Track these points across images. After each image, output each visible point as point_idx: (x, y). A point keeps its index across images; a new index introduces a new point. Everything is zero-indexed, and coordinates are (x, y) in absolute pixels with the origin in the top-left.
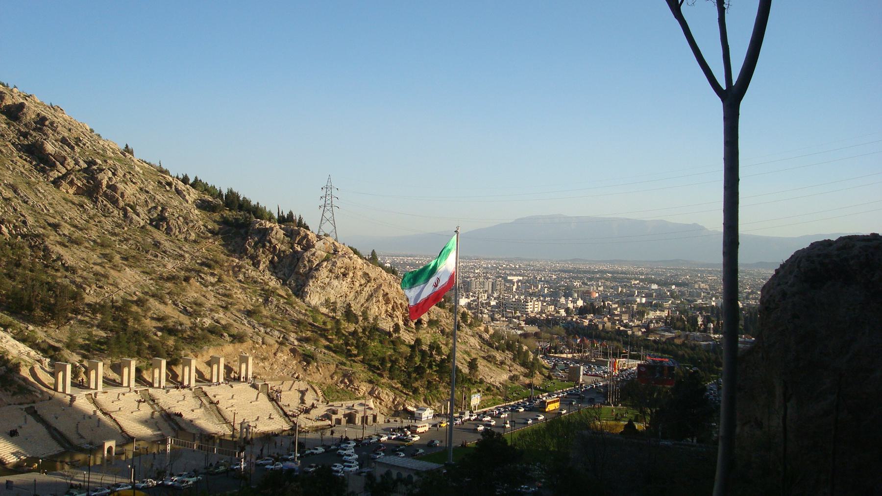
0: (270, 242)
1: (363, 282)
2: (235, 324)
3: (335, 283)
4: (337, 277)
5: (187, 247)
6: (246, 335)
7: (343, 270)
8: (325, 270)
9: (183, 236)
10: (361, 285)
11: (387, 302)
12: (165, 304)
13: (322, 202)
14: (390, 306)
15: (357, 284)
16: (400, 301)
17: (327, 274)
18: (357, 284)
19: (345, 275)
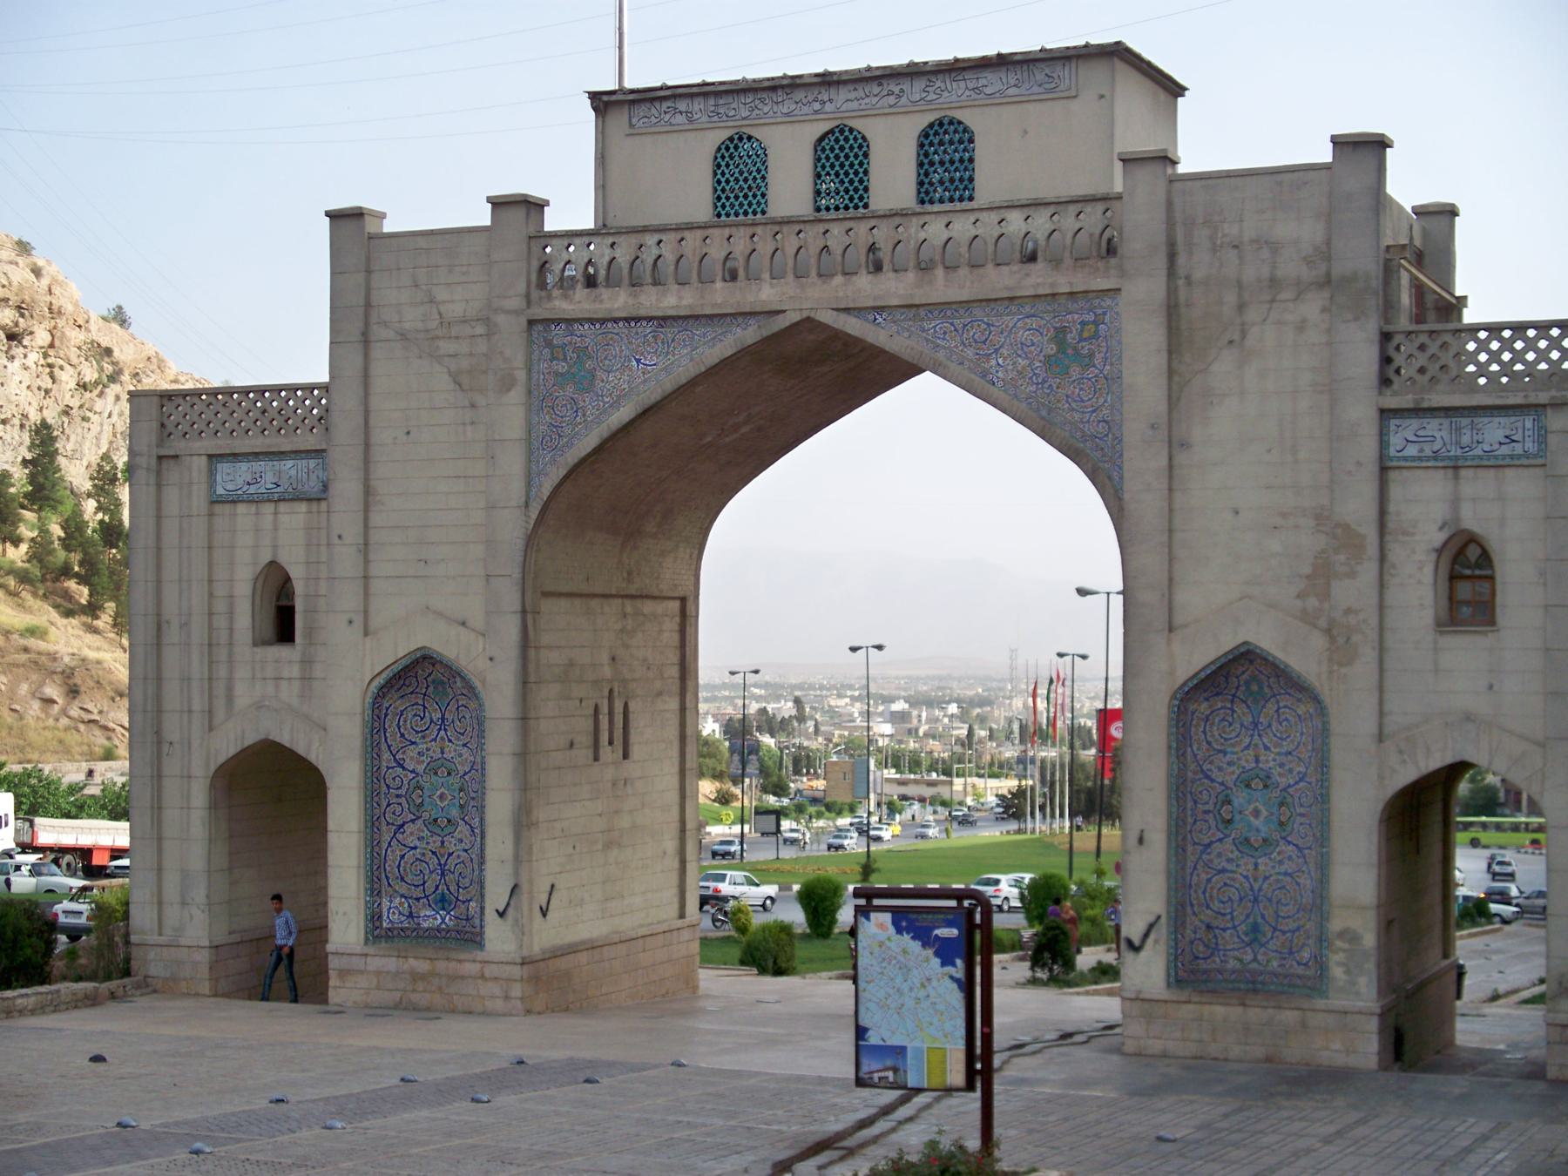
1: (90, 374)
15: (67, 378)
18: (67, 378)
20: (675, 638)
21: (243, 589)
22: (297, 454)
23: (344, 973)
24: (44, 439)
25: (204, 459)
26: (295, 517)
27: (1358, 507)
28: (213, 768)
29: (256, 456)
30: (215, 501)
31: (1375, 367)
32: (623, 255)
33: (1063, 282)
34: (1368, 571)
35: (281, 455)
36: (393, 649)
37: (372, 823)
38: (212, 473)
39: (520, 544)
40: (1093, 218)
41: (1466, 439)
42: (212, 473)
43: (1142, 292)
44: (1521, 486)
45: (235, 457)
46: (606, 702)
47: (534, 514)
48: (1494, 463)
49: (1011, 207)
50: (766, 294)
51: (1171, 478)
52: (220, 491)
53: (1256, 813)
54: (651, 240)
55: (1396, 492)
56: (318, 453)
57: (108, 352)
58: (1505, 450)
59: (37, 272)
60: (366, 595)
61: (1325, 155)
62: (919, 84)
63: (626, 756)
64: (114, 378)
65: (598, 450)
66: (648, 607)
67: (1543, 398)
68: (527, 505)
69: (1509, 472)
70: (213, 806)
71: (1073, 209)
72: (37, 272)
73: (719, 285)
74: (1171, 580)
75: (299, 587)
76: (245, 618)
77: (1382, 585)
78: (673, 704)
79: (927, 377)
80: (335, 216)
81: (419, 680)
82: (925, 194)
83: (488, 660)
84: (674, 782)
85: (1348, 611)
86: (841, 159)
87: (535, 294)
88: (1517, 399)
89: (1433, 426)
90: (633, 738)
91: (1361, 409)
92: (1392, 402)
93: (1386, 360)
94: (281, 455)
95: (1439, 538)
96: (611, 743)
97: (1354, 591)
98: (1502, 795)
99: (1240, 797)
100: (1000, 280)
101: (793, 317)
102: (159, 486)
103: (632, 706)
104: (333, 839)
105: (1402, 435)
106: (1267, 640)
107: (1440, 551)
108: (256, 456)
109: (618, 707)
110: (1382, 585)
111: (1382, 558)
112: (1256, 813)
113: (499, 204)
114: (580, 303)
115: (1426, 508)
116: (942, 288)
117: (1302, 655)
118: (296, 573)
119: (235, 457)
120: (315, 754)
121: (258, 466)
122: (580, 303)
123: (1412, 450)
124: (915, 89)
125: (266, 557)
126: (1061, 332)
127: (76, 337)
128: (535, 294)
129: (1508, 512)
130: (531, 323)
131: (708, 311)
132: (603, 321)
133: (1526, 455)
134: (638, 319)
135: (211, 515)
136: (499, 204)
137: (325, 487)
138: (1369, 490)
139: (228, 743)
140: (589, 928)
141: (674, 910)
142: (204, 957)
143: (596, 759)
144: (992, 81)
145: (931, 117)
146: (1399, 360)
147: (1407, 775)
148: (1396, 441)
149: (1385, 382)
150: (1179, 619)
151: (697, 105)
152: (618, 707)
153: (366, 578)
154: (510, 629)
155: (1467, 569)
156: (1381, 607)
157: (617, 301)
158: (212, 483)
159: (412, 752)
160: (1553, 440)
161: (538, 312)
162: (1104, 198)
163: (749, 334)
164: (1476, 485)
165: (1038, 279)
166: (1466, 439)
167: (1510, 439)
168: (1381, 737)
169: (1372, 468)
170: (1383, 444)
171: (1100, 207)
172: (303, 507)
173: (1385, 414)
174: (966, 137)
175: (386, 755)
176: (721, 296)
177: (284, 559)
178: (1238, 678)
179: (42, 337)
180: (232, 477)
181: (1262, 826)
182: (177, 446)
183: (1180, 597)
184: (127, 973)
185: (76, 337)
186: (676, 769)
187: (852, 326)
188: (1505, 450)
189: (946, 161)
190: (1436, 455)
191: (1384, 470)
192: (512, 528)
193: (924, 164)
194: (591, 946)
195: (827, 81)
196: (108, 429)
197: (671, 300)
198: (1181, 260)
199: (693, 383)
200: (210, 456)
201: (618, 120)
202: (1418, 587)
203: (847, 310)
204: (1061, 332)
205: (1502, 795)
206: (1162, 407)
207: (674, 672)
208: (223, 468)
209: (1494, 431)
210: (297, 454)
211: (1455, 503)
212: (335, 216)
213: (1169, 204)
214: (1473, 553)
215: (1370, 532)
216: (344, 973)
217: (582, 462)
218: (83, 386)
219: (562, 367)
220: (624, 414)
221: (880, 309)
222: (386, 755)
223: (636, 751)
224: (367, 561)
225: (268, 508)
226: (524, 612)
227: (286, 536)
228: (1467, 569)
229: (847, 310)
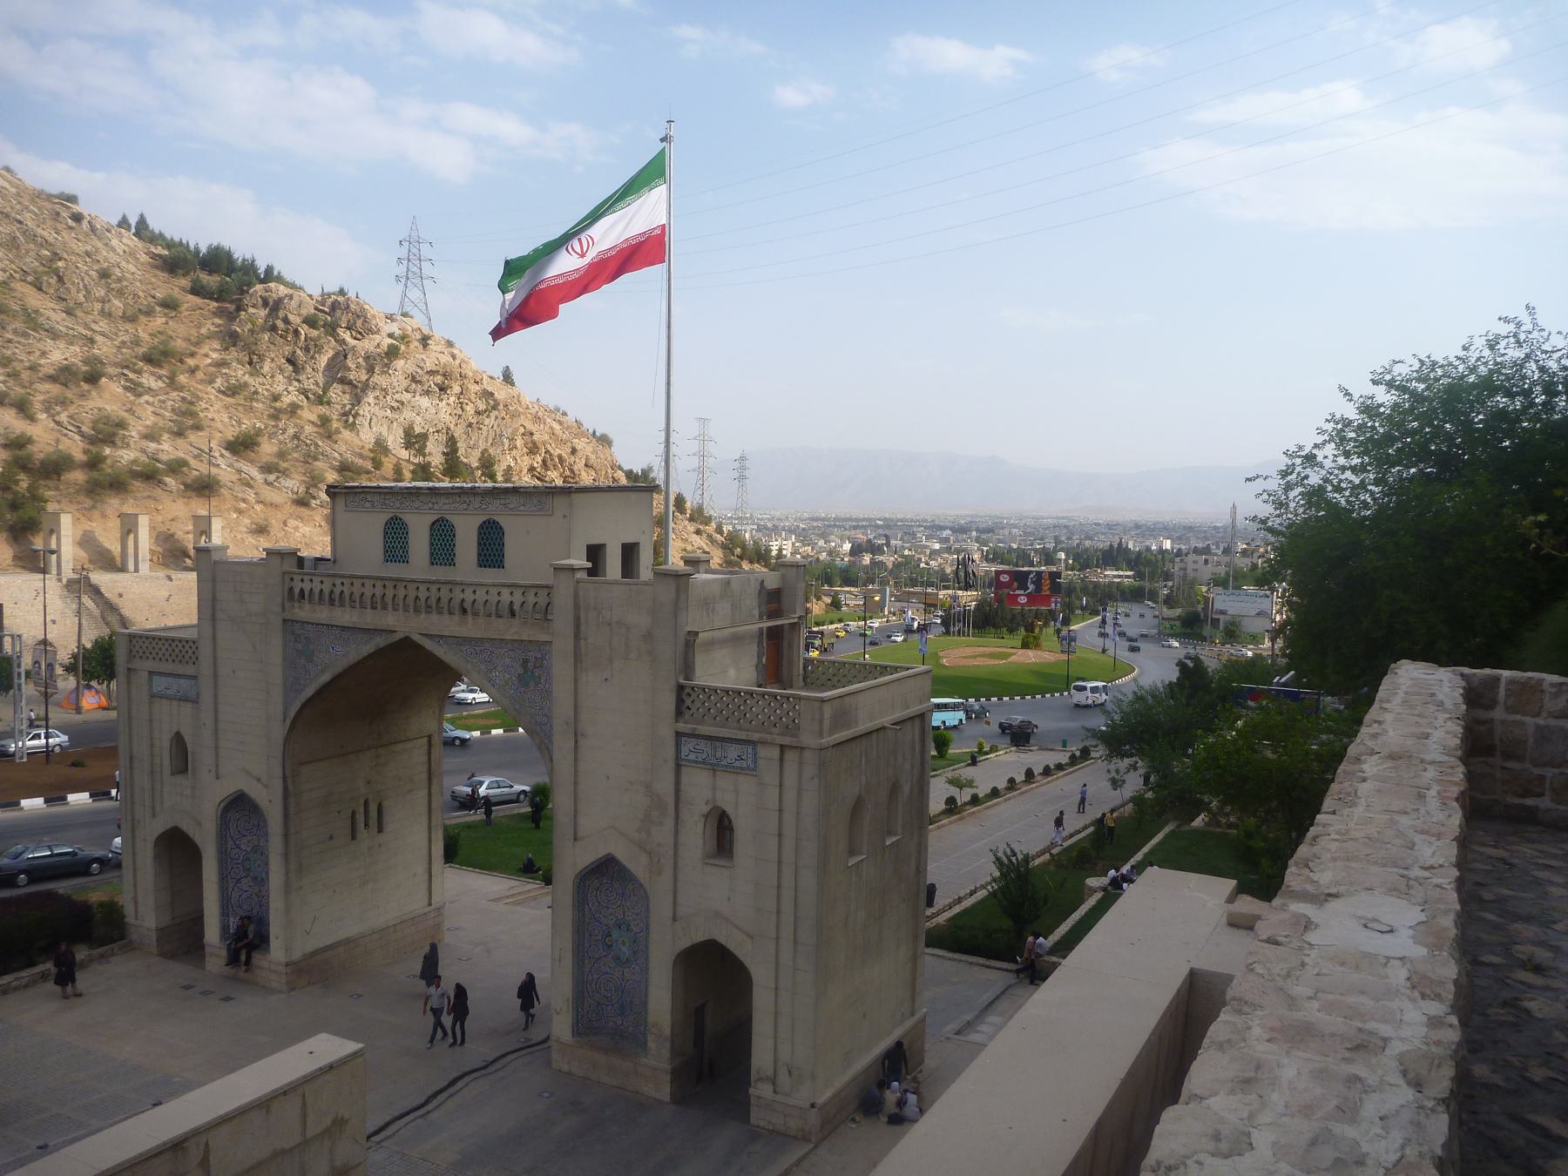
0: (286, 321)
1: (482, 407)
2: (193, 462)
3: (424, 402)
4: (427, 393)
5: (103, 325)
6: (218, 482)
7: (439, 379)
8: (401, 377)
9: (98, 306)
10: (478, 413)
11: (533, 449)
12: (31, 418)
13: (402, 270)
14: (539, 459)
15: (470, 409)
16: (558, 452)
17: (405, 383)
18: (470, 409)
19: (442, 389)
20: (425, 758)
21: (166, 744)
23: (212, 955)
24: (452, 442)
26: (187, 709)
27: (665, 786)
29: (169, 675)
30: (153, 696)
31: (673, 707)
32: (327, 588)
33: (527, 634)
34: (669, 823)
35: (179, 676)
36: (227, 788)
37: (223, 878)
38: (150, 680)
39: (281, 741)
40: (542, 599)
41: (718, 755)
42: (150, 680)
43: (562, 646)
44: (746, 784)
45: (160, 674)
46: (362, 809)
48: (731, 769)
49: (504, 586)
50: (390, 620)
51: (576, 753)
53: (624, 943)
54: (338, 582)
55: (684, 779)
56: (194, 678)
57: (492, 394)
58: (737, 764)
59: (454, 357)
60: (217, 755)
62: (478, 499)
63: (380, 830)
64: (494, 408)
65: (314, 696)
66: (400, 747)
67: (756, 736)
69: (741, 778)
70: (157, 857)
71: (533, 591)
72: (454, 357)
73: (369, 611)
74: (576, 811)
77: (676, 832)
78: (424, 793)
81: (239, 806)
83: (269, 799)
84: (425, 834)
85: (659, 845)
86: (442, 535)
87: (287, 604)
89: (702, 744)
90: (386, 819)
91: (666, 731)
92: (681, 727)
93: (680, 701)
94: (179, 676)
95: (706, 809)
96: (366, 825)
97: (662, 834)
99: (615, 934)
101: (402, 636)
102: (129, 683)
103: (386, 804)
104: (205, 885)
105: (688, 746)
106: (621, 856)
107: (706, 816)
108: (169, 675)
109: (373, 808)
110: (676, 832)
111: (677, 818)
112: (624, 943)
114: (304, 612)
117: (637, 865)
118: (188, 739)
119: (160, 674)
120: (197, 839)
122: (304, 612)
123: (692, 757)
124: (476, 502)
125: (175, 730)
126: (525, 662)
127: (474, 388)
128: (287, 604)
129: (742, 798)
133: (748, 768)
135: (151, 703)
138: (671, 778)
139: (159, 826)
140: (351, 929)
141: (426, 902)
142: (154, 935)
143: (353, 838)
144: (514, 501)
145: (485, 518)
146: (688, 702)
149: (679, 713)
150: (581, 833)
151: (376, 498)
152: (373, 808)
153: (217, 748)
154: (278, 785)
155: (722, 830)
156: (676, 844)
157: (322, 614)
159: (245, 840)
160: (761, 763)
161: (288, 616)
162: (547, 587)
163: (381, 641)
164: (725, 781)
165: (511, 630)
166: (718, 755)
168: (674, 919)
169: (671, 764)
171: (546, 591)
172: (190, 705)
173: (678, 735)
175: (230, 842)
176: (369, 619)
179: (457, 389)
180: (160, 684)
181: (625, 951)
182: (137, 664)
183: (582, 821)
184: (122, 938)
185: (474, 388)
186: (426, 826)
187: (428, 644)
188: (737, 764)
189: (491, 547)
190: (704, 762)
191: (678, 767)
192: (279, 732)
193: (482, 543)
194: (348, 941)
196: (492, 434)
197: (346, 617)
198: (583, 628)
199: (359, 663)
201: (340, 501)
202: (696, 837)
203: (426, 635)
204: (525, 662)
206: (572, 714)
207: (424, 776)
208: (156, 678)
209: (733, 752)
211: (714, 788)
213: (576, 596)
215: (670, 800)
216: (212, 955)
217: (310, 700)
218: (478, 413)
219: (299, 646)
220: (326, 677)
221: (442, 637)
222: (230, 842)
223: (389, 826)
224: (217, 740)
225: (175, 703)
226: (285, 778)
228: (722, 830)
229: (426, 635)
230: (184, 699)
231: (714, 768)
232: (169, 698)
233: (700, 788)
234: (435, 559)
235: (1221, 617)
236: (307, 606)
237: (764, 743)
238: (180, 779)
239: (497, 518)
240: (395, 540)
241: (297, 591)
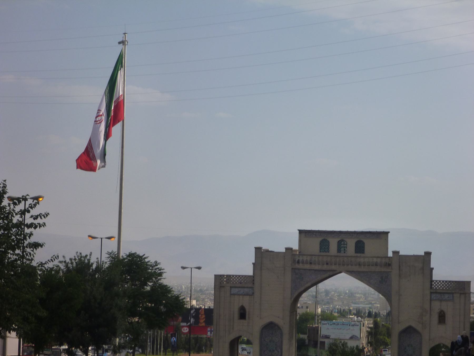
22: (247, 287)
25: (229, 288)
26: (247, 298)
28: (230, 341)
29: (239, 287)
30: (231, 294)
33: (383, 269)
36: (266, 321)
38: (231, 290)
47: (293, 299)
49: (374, 257)
52: (232, 293)
54: (314, 257)
61: (423, 254)
67: (453, 292)
68: (291, 298)
75: (247, 310)
76: (236, 315)
79: (343, 274)
80: (256, 248)
81: (271, 327)
82: (356, 252)
88: (450, 292)
92: (432, 291)
94: (244, 287)
98: (307, 341)
100: (373, 269)
105: (434, 296)
106: (413, 325)
108: (239, 287)
111: (430, 314)
113: (287, 249)
114: (301, 266)
115: (437, 306)
116: (362, 269)
117: (419, 327)
118: (247, 308)
121: (240, 289)
122: (301, 266)
123: (435, 298)
125: (241, 305)
129: (448, 307)
130: (292, 269)
131: (324, 269)
132: (305, 269)
134: (311, 270)
136: (287, 249)
137: (253, 293)
145: (358, 240)
147: (433, 345)
148: (433, 297)
157: (307, 266)
158: (231, 292)
165: (378, 269)
167: (449, 297)
168: (430, 340)
170: (431, 297)
173: (431, 293)
174: (364, 243)
177: (244, 305)
178: (409, 331)
180: (235, 291)
189: (360, 247)
191: (431, 300)
195: (341, 232)
197: (317, 267)
200: (231, 287)
202: (435, 318)
205: (307, 341)
208: (233, 289)
209: (446, 296)
210: (247, 287)
212: (256, 248)
214: (442, 313)
221: (353, 271)
225: (241, 297)
227: (245, 301)
230: (247, 295)
231: (441, 301)
232: (239, 295)
233: (437, 306)
234: (339, 251)
235: (327, 341)
236: (301, 264)
237: (456, 293)
238: (242, 321)
239: (362, 240)
240: (324, 245)
241: (297, 260)
